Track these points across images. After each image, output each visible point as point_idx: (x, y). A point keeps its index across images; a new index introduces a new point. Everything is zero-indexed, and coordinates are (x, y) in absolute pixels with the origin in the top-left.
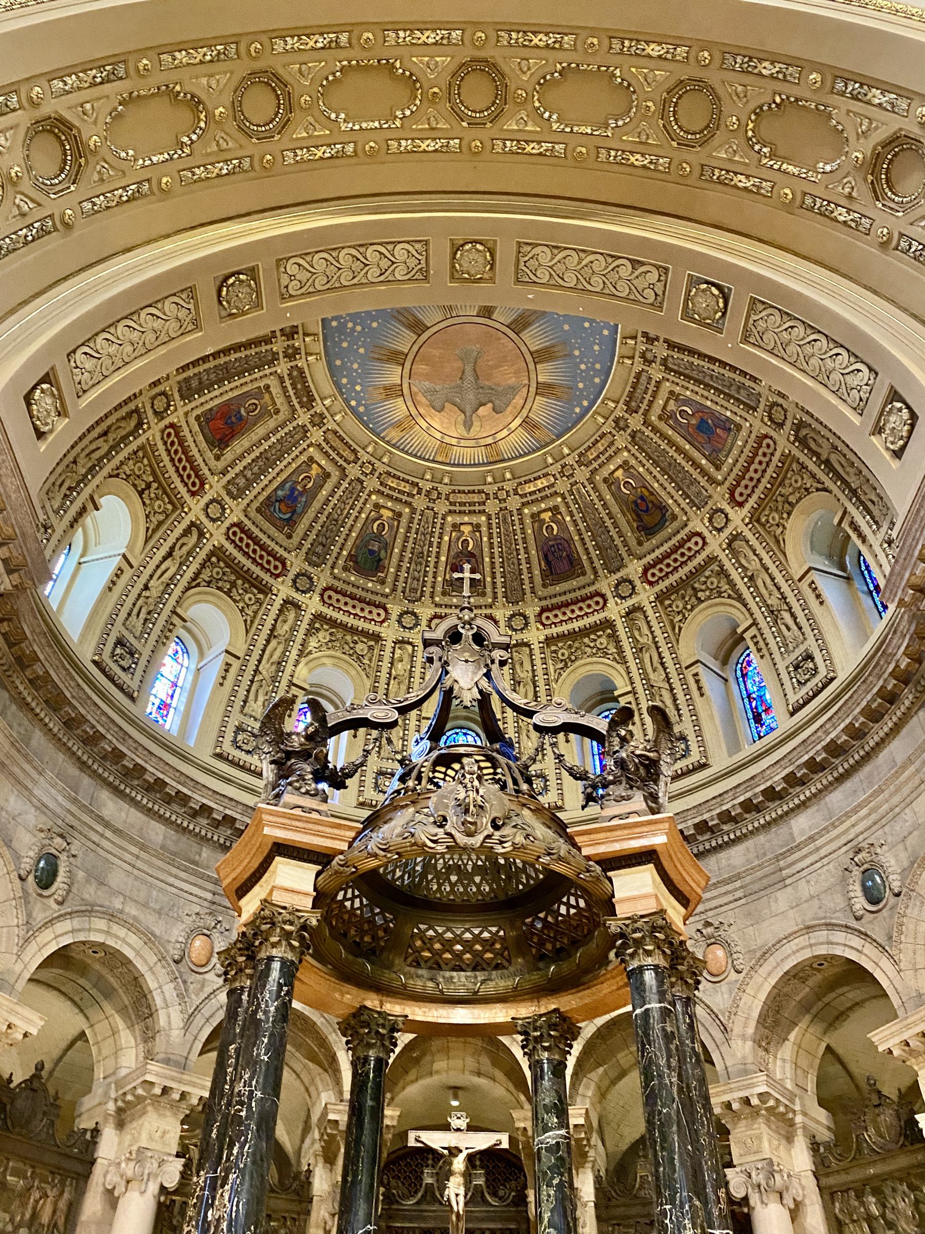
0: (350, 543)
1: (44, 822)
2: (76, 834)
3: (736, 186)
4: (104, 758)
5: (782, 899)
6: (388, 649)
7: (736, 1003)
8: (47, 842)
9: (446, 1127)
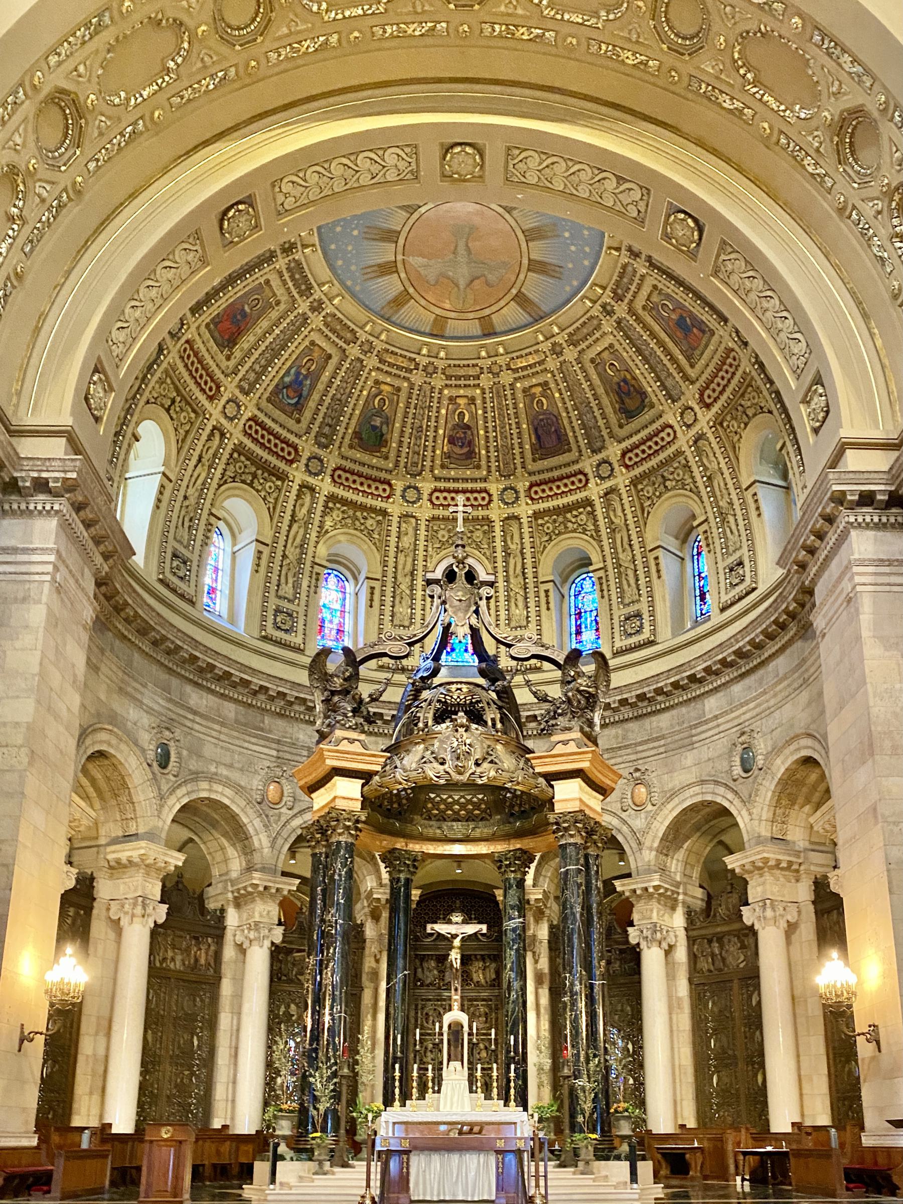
1: (154, 721)
2: (175, 724)
3: (720, 105)
4: (184, 662)
5: (689, 758)
6: (395, 524)
7: (649, 826)
8: (159, 735)
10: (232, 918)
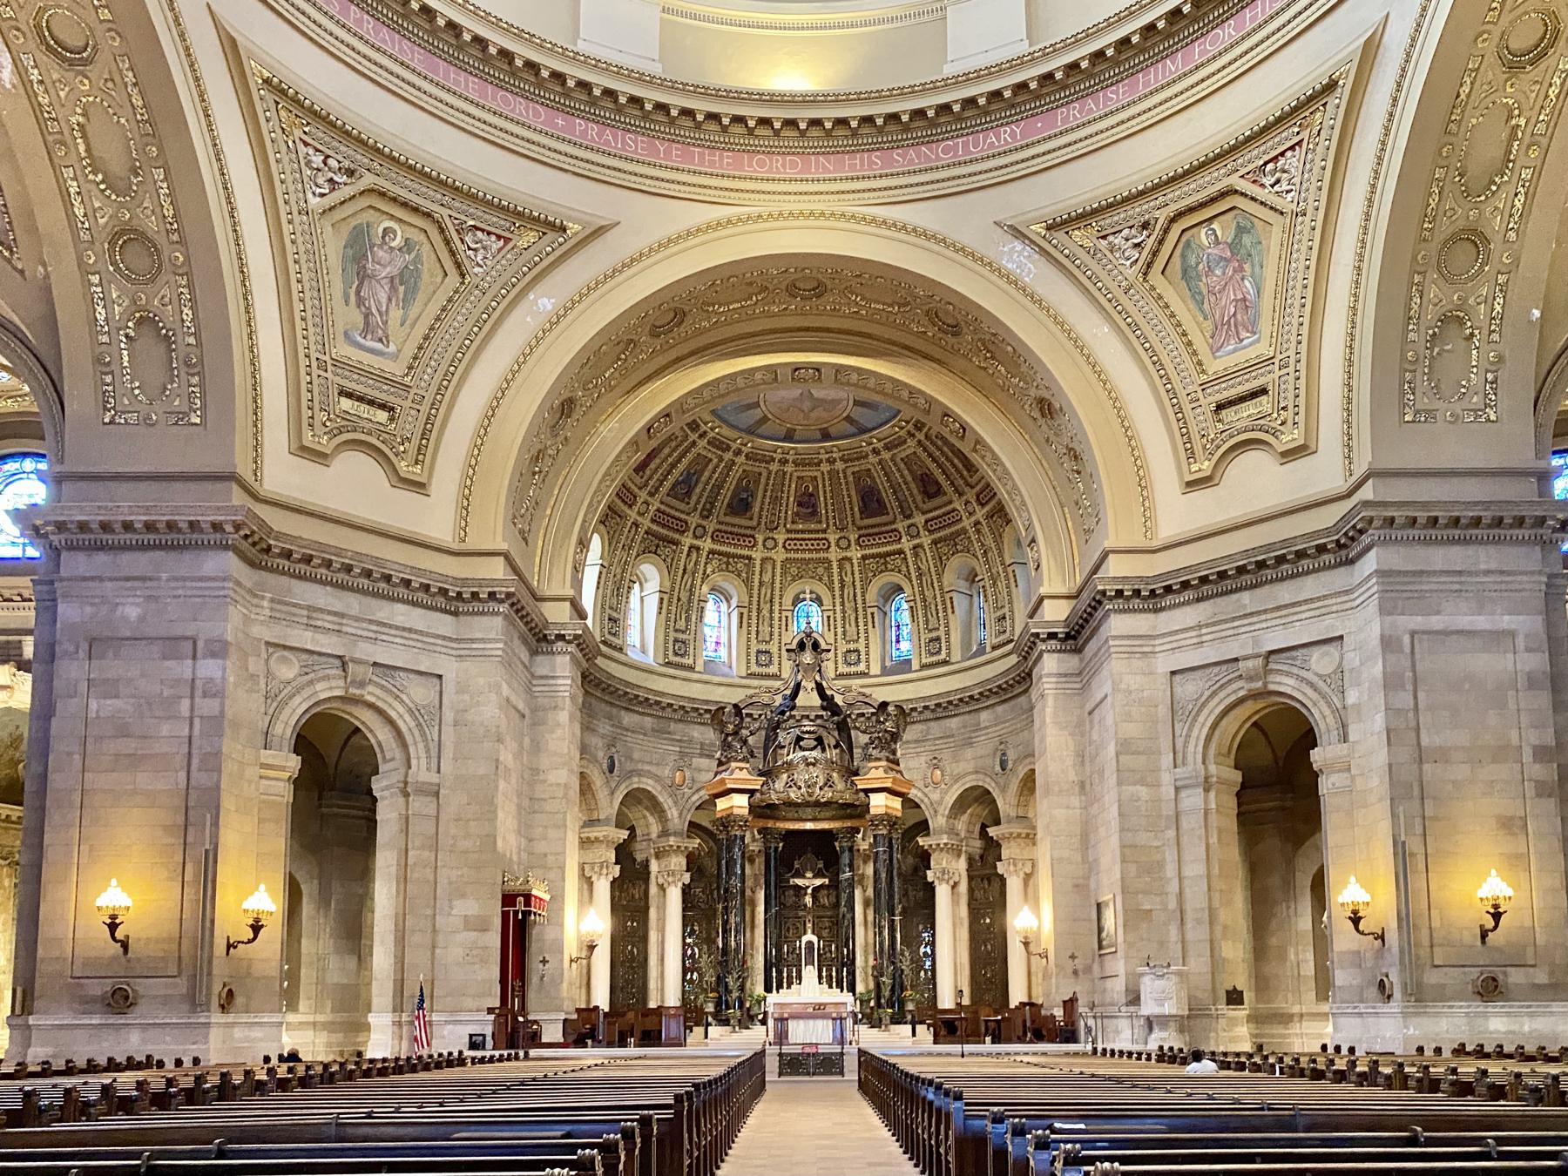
5: (969, 753)
7: (942, 798)
9: (804, 877)
10: (654, 866)
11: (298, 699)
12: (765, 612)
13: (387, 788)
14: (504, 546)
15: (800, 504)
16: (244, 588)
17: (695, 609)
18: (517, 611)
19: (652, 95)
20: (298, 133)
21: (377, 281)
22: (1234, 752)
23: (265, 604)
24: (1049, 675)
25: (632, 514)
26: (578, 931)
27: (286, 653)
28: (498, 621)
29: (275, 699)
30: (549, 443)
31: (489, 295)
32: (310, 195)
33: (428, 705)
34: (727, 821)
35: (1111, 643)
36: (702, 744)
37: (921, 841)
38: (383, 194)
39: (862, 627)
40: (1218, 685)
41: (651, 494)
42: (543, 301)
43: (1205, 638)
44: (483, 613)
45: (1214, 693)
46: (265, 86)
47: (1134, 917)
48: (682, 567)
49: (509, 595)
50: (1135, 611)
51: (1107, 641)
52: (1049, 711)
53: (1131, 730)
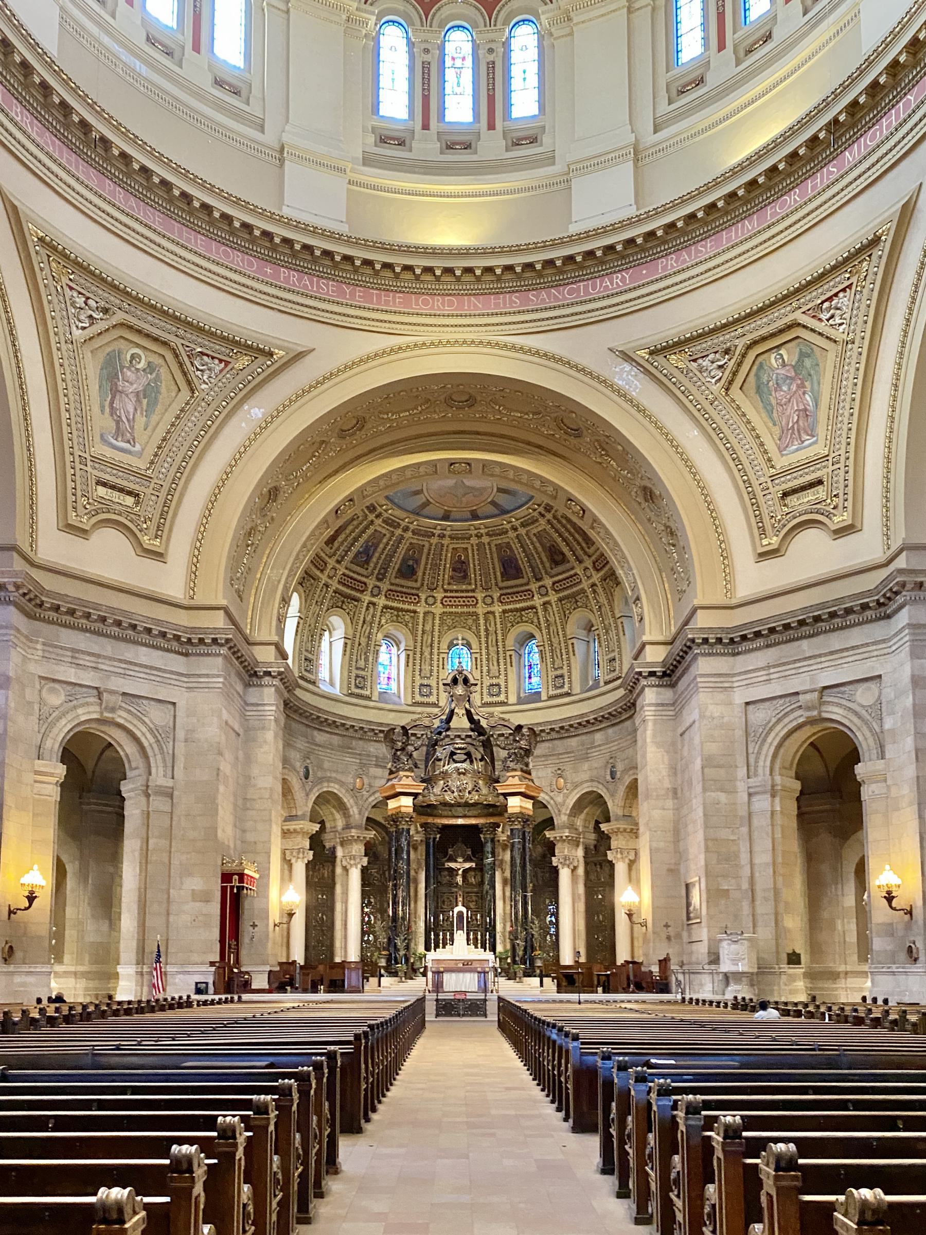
0: (399, 562)
5: (586, 766)
7: (564, 801)
9: (456, 861)
10: (340, 852)
11: (63, 721)
12: (427, 654)
13: (132, 790)
14: (224, 602)
15: (454, 570)
16: (22, 634)
17: (372, 652)
18: (234, 653)
19: (341, 249)
20: (65, 280)
21: (127, 395)
22: (795, 766)
23: (39, 646)
24: (649, 705)
25: (324, 578)
26: (281, 902)
27: (57, 686)
28: (220, 660)
29: (46, 720)
30: (259, 522)
31: (213, 405)
32: (74, 328)
33: (165, 726)
34: (396, 818)
35: (699, 680)
36: (376, 757)
37: (548, 834)
38: (130, 328)
39: (502, 667)
40: (783, 713)
41: (338, 562)
42: (255, 411)
43: (772, 676)
44: (208, 655)
45: (779, 720)
46: (40, 243)
47: (715, 895)
48: (362, 619)
49: (228, 641)
50: (717, 654)
51: (695, 678)
52: (649, 733)
53: (713, 748)
